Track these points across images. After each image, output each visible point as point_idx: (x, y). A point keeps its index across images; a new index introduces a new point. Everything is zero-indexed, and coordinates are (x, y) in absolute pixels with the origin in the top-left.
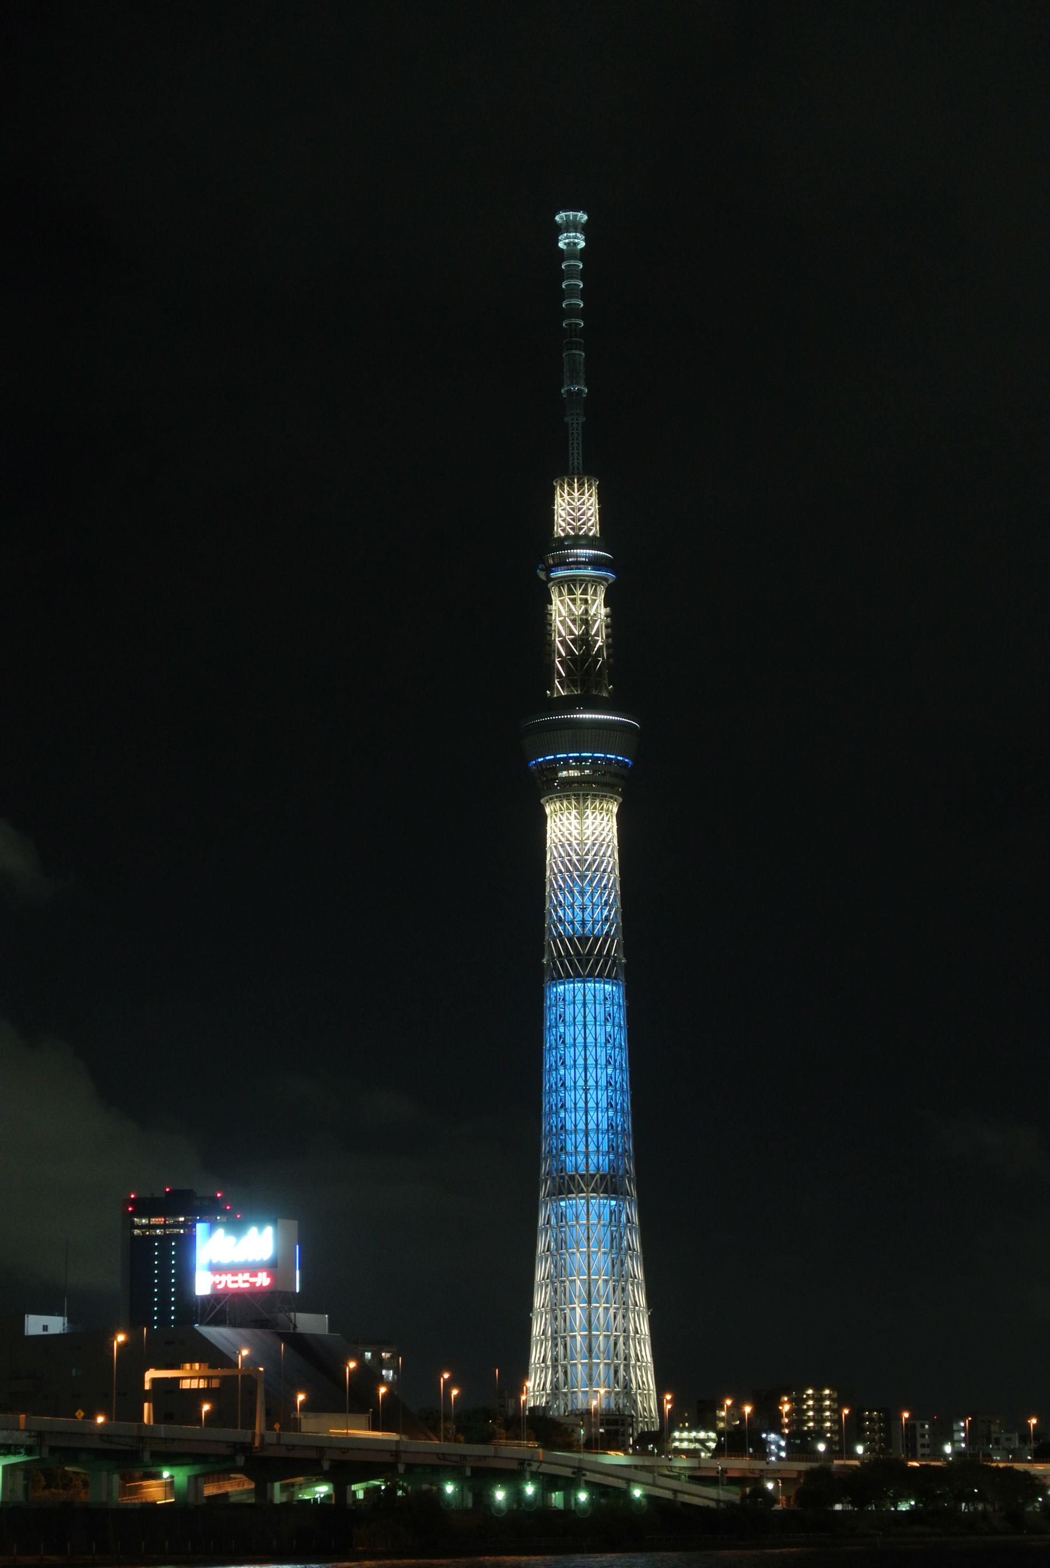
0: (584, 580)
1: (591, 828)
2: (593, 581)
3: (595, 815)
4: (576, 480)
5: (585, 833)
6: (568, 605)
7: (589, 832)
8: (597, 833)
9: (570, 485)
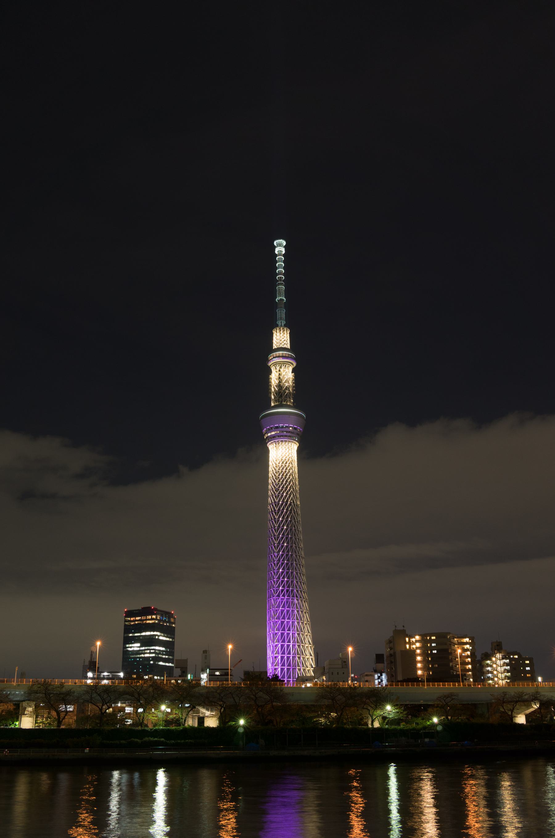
0: (279, 363)
1: (281, 453)
2: (285, 363)
3: (282, 448)
4: (278, 329)
5: (279, 455)
6: (275, 374)
7: (280, 455)
8: (283, 455)
9: (276, 331)
